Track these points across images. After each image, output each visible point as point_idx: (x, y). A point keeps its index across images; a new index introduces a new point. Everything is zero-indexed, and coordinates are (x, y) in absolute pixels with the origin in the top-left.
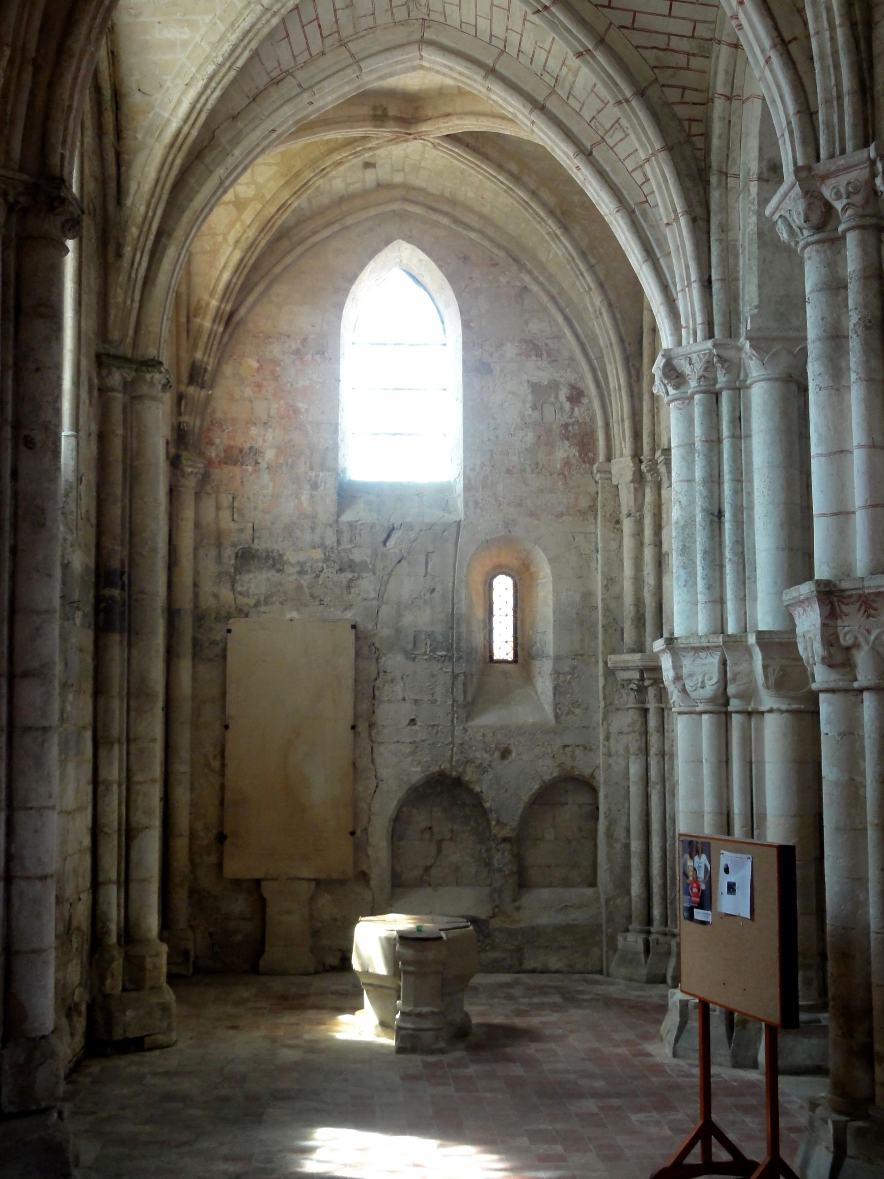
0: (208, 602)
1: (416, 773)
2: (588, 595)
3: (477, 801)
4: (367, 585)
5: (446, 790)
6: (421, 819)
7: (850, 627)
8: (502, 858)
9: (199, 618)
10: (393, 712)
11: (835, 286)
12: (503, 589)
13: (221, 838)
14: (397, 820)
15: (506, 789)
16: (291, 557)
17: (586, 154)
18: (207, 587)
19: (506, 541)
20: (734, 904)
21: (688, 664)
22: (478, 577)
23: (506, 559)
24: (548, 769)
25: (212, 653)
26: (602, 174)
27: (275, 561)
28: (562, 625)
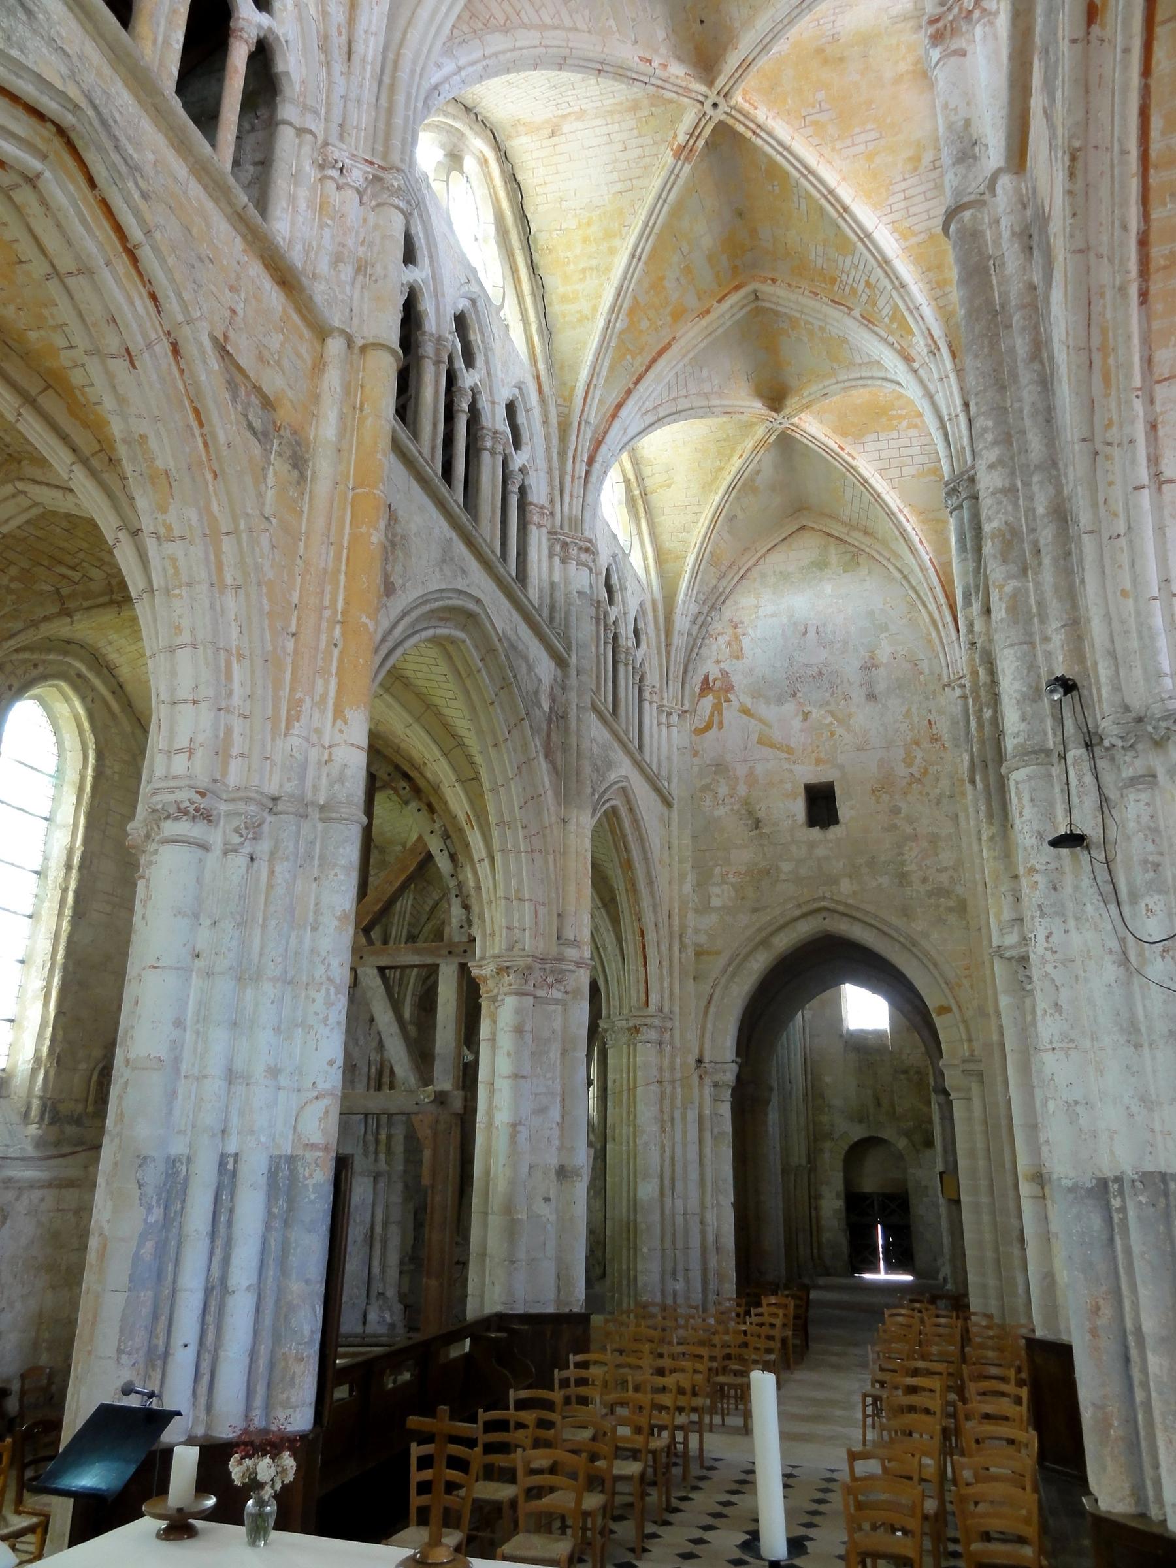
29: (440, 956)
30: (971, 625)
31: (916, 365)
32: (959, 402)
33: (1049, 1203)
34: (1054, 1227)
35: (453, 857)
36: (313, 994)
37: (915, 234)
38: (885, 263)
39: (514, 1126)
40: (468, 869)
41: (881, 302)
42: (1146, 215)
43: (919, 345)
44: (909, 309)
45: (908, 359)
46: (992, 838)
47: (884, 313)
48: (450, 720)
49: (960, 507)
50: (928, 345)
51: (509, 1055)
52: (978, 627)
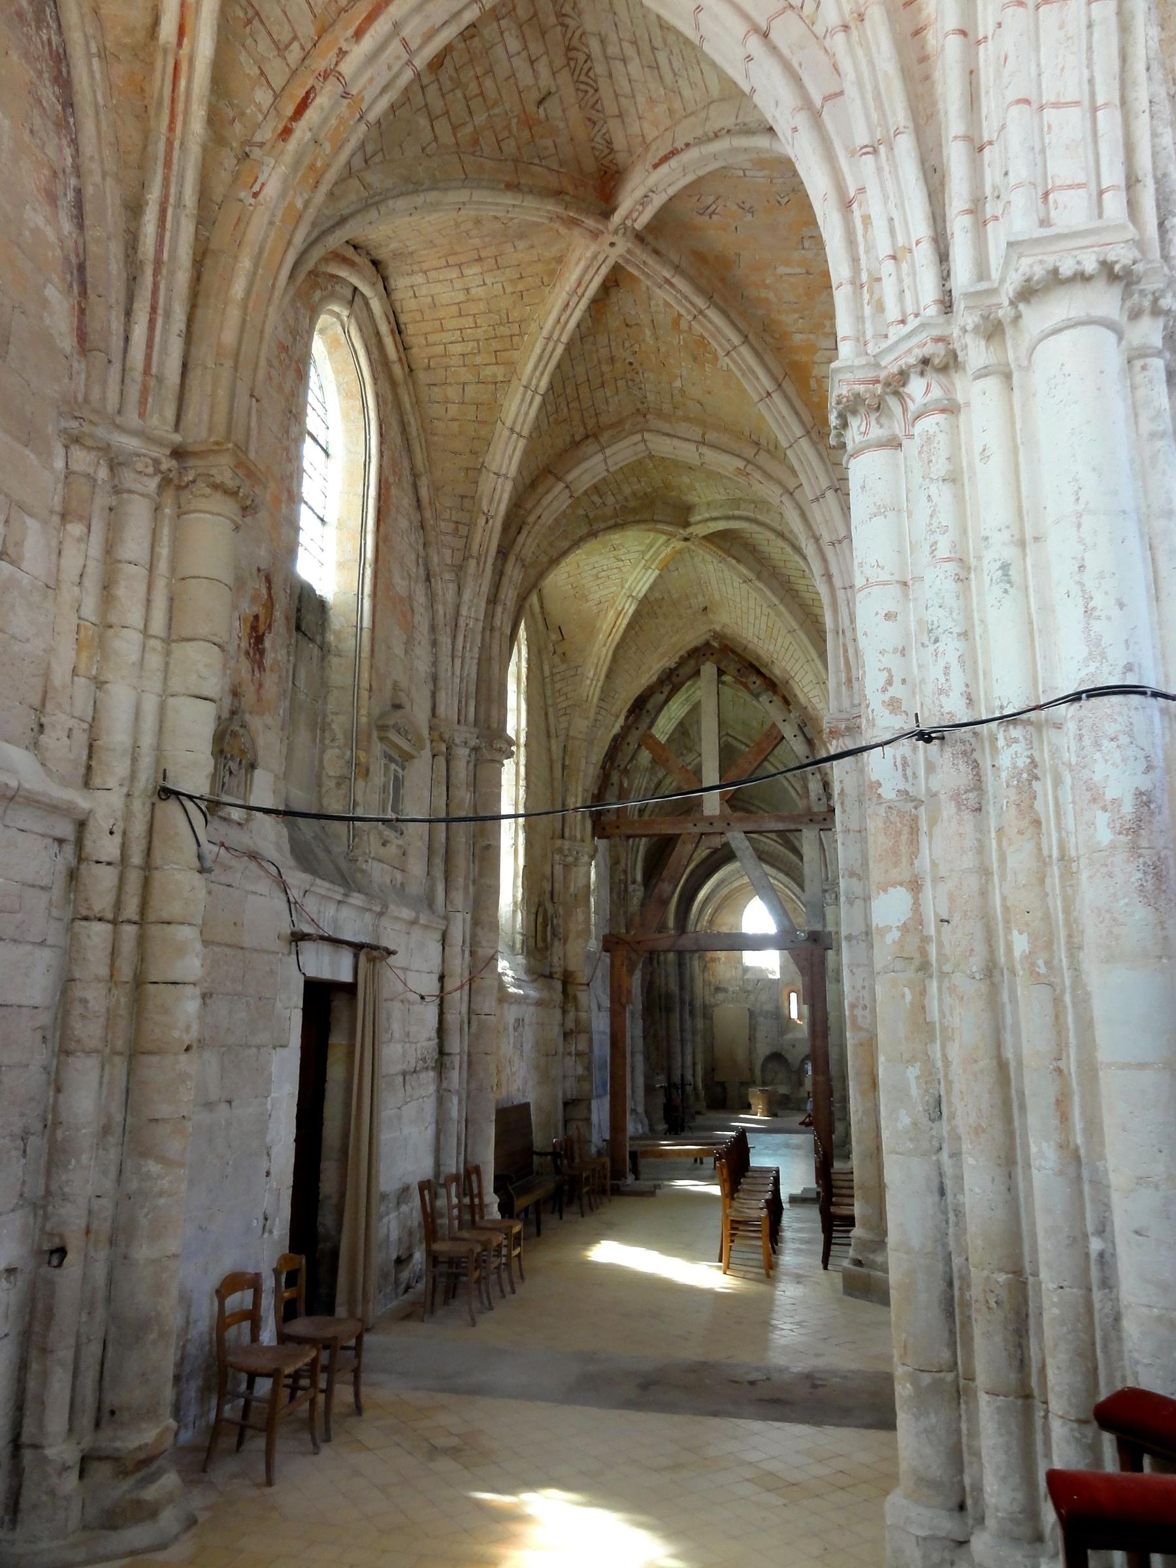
0: (707, 1002)
3: (786, 1061)
4: (752, 997)
5: (776, 1057)
6: (770, 1066)
9: (705, 1007)
10: (760, 1035)
13: (713, 1070)
16: (731, 989)
18: (707, 998)
22: (785, 993)
23: (793, 988)
25: (708, 1015)
27: (726, 991)
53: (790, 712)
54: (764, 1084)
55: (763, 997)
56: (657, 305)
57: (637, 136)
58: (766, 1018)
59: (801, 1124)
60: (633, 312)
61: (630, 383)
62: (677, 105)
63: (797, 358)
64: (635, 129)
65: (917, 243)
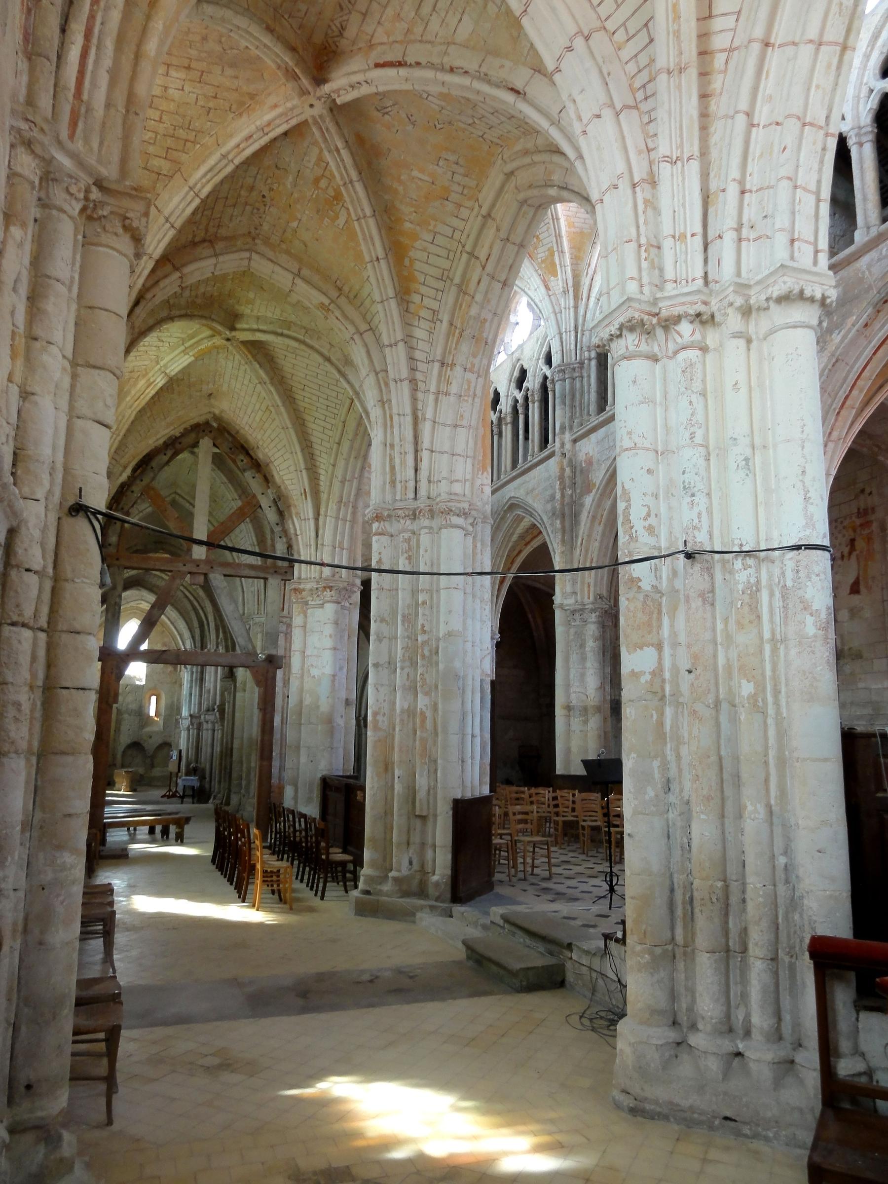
1: (129, 741)
2: (173, 702)
5: (136, 746)
7: (194, 720)
8: (148, 761)
11: (197, 672)
12: (154, 699)
14: (124, 752)
15: (151, 745)
17: (172, 623)
19: (155, 688)
20: (174, 758)
21: (184, 721)
22: (147, 696)
24: (160, 741)
26: (175, 628)
28: (166, 708)
29: (268, 573)
30: (563, 445)
31: (551, 293)
32: (572, 325)
33: (572, 718)
34: (573, 728)
35: (281, 513)
36: (484, 606)
37: (574, 227)
38: (558, 236)
39: (334, 676)
40: (290, 522)
41: (540, 250)
42: (851, 391)
43: (557, 284)
44: (560, 264)
45: (547, 288)
46: (563, 552)
47: (539, 256)
48: (310, 431)
49: (564, 380)
50: (563, 287)
51: (331, 636)
52: (568, 446)
53: (269, 488)
54: (123, 766)
55: (130, 698)
56: (309, 161)
57: (367, 34)
58: (130, 715)
59: (162, 797)
60: (287, 159)
61: (255, 211)
62: (418, 30)
63: (402, 239)
64: (369, 28)
65: (693, 235)
